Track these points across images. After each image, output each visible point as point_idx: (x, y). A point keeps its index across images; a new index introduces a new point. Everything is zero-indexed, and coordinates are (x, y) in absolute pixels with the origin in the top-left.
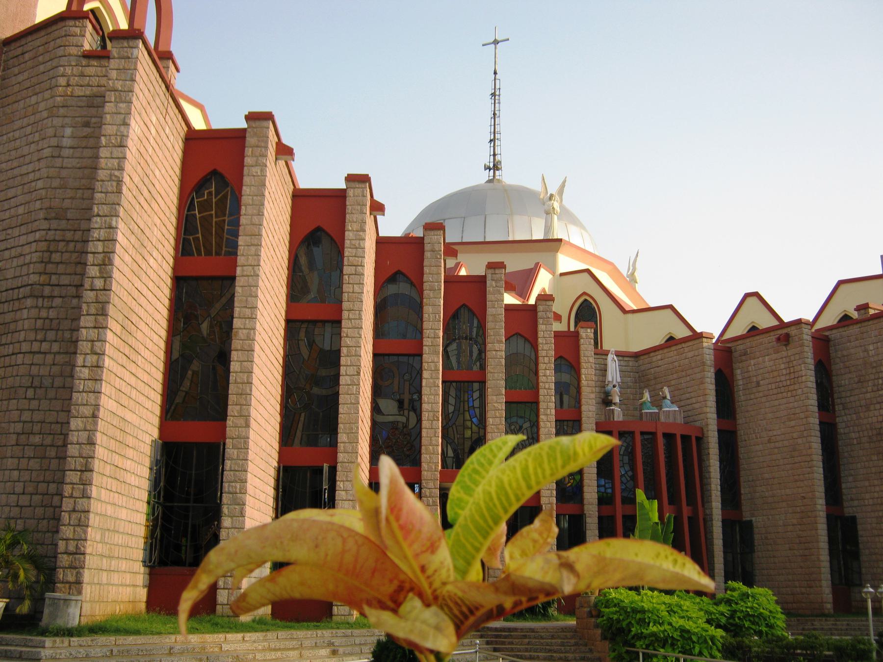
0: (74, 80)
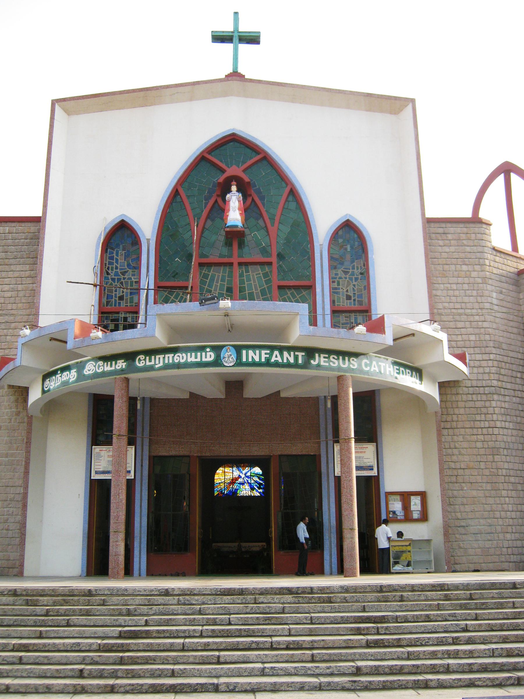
0: (492, 264)
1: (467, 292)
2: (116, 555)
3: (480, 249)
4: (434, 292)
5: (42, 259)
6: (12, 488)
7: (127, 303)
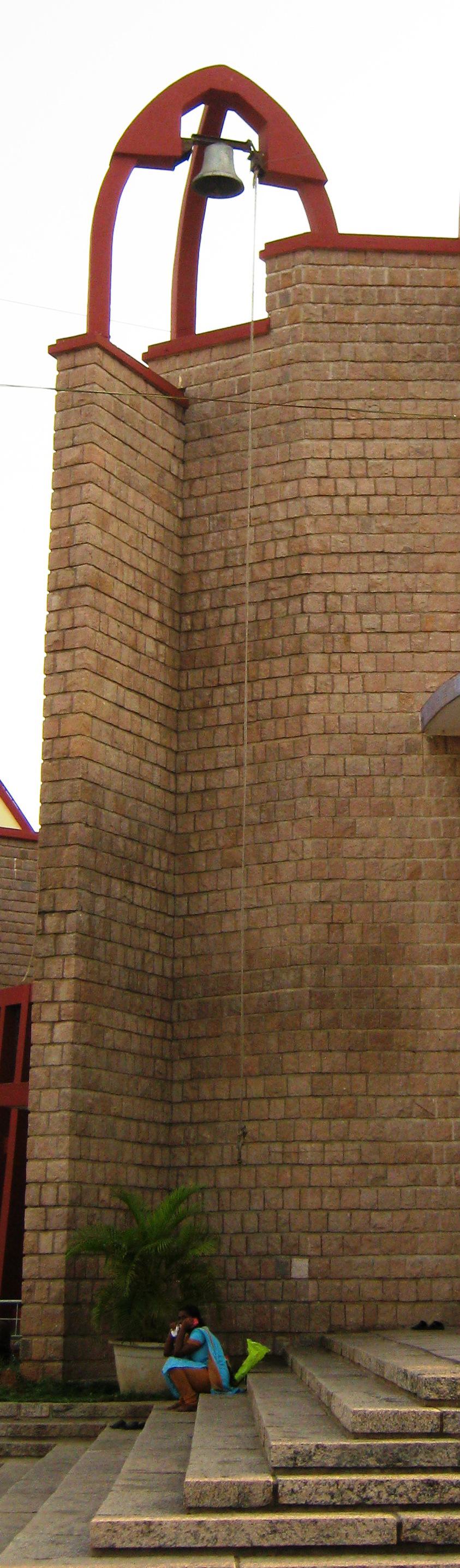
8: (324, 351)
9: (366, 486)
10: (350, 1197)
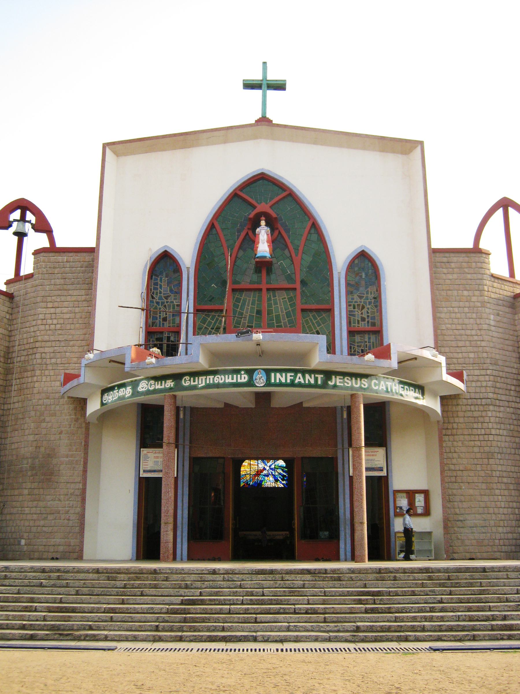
1: (468, 314)
2: (166, 543)
3: (480, 276)
4: (438, 315)
5: (96, 286)
6: (72, 484)
7: (169, 323)
8: (46, 282)
9: (55, 322)
10: (38, 523)
